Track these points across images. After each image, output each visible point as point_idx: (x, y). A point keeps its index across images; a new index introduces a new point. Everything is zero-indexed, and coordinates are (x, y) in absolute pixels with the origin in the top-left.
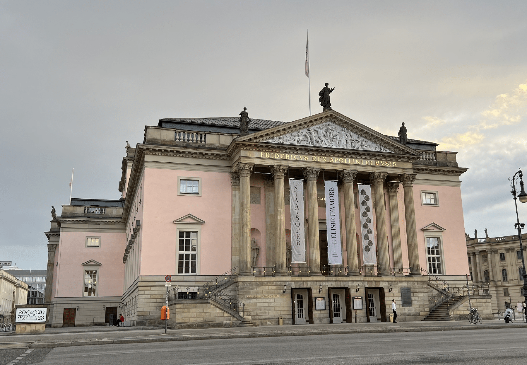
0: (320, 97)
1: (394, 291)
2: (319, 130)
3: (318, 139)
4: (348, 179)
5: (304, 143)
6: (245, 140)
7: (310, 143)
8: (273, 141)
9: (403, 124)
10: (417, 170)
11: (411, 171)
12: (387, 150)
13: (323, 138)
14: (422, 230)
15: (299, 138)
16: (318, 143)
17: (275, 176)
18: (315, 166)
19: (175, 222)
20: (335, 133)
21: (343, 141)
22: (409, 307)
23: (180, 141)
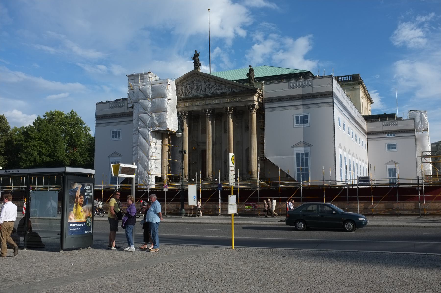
2: (187, 85)
9: (250, 66)
12: (234, 89)
13: (190, 90)
20: (199, 84)
21: (202, 89)
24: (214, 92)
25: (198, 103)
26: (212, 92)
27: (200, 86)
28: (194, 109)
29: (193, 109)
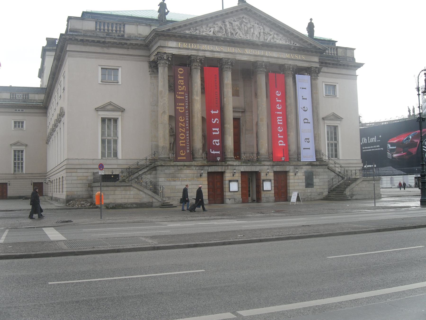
1: (299, 174)
3: (233, 31)
4: (261, 70)
5: (220, 35)
6: (164, 31)
7: (225, 35)
8: (190, 32)
10: (323, 63)
11: (316, 64)
13: (238, 31)
14: (323, 119)
15: (214, 29)
16: (232, 35)
17: (192, 66)
18: (230, 57)
19: (97, 109)
22: (311, 188)
23: (100, 31)
24: (272, 41)
25: (248, 51)
26: (269, 40)
27: (251, 28)
28: (244, 58)
29: (242, 58)
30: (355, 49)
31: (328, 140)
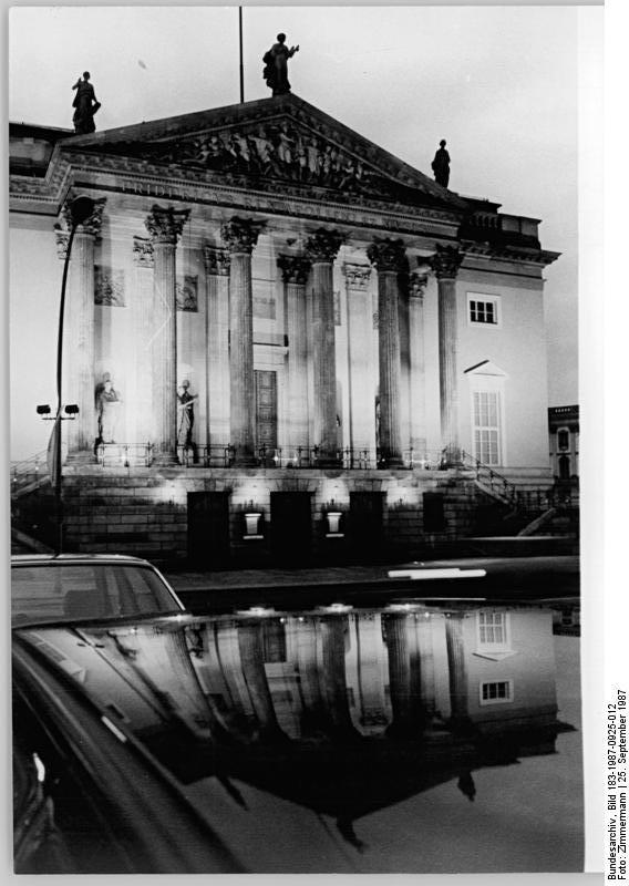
0: (265, 65)
9: (443, 143)
30: (539, 221)
31: (478, 423)
